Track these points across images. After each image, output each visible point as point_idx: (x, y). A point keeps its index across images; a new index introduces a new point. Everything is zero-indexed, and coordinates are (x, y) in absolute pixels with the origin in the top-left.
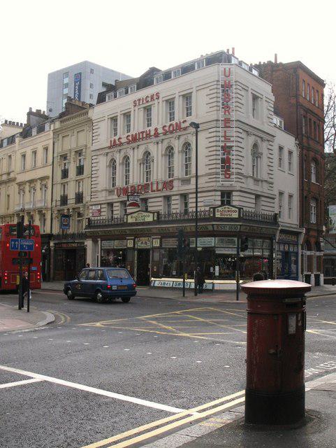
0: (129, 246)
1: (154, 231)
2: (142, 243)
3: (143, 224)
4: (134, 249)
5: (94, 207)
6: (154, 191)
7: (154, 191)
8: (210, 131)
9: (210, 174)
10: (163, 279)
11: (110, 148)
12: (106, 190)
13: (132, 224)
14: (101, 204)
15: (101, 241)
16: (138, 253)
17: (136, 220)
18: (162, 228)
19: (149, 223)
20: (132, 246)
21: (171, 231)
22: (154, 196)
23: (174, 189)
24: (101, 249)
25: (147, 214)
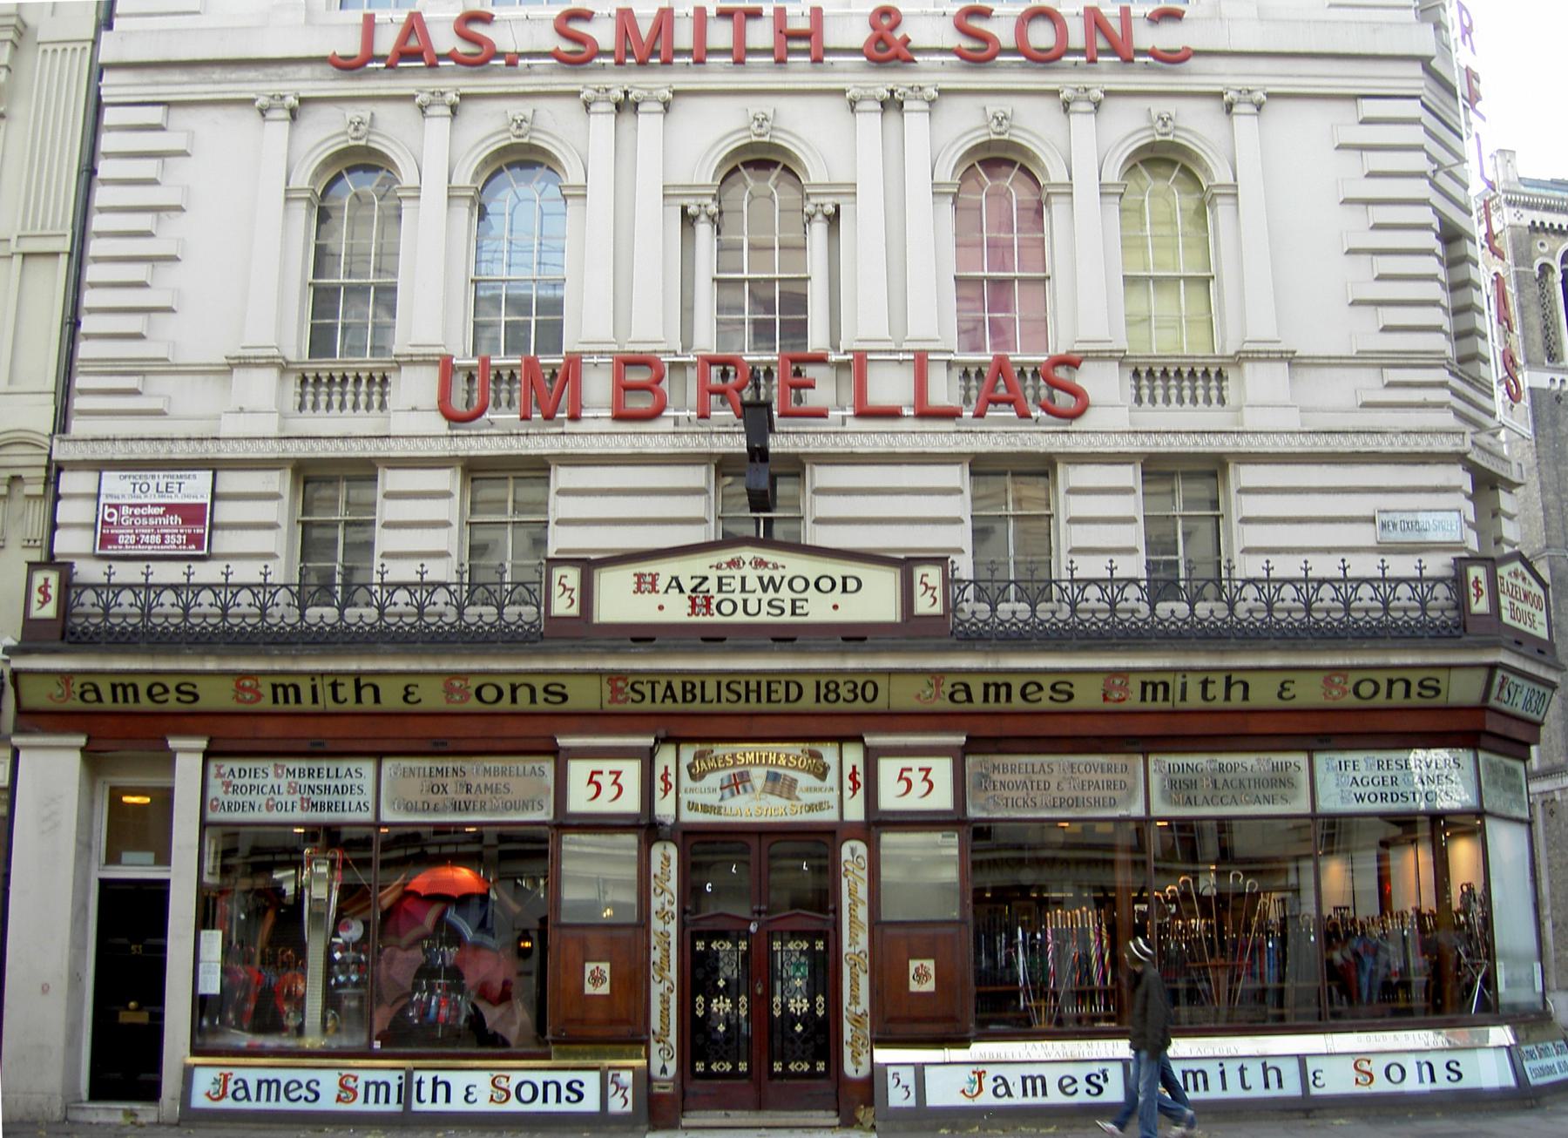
0: (580, 801)
1: (902, 696)
2: (738, 783)
3: (784, 638)
4: (647, 828)
5: (116, 485)
6: (893, 414)
7: (893, 414)
8: (1370, 108)
9: (1362, 360)
10: (980, 1050)
11: (348, 66)
12: (284, 368)
13: (643, 637)
14: (215, 466)
15: (208, 755)
16: (691, 870)
17: (700, 600)
18: (998, 685)
19: (854, 636)
20: (630, 803)
21: (1088, 696)
22: (881, 445)
23: (1076, 425)
24: (204, 825)
25: (837, 569)
